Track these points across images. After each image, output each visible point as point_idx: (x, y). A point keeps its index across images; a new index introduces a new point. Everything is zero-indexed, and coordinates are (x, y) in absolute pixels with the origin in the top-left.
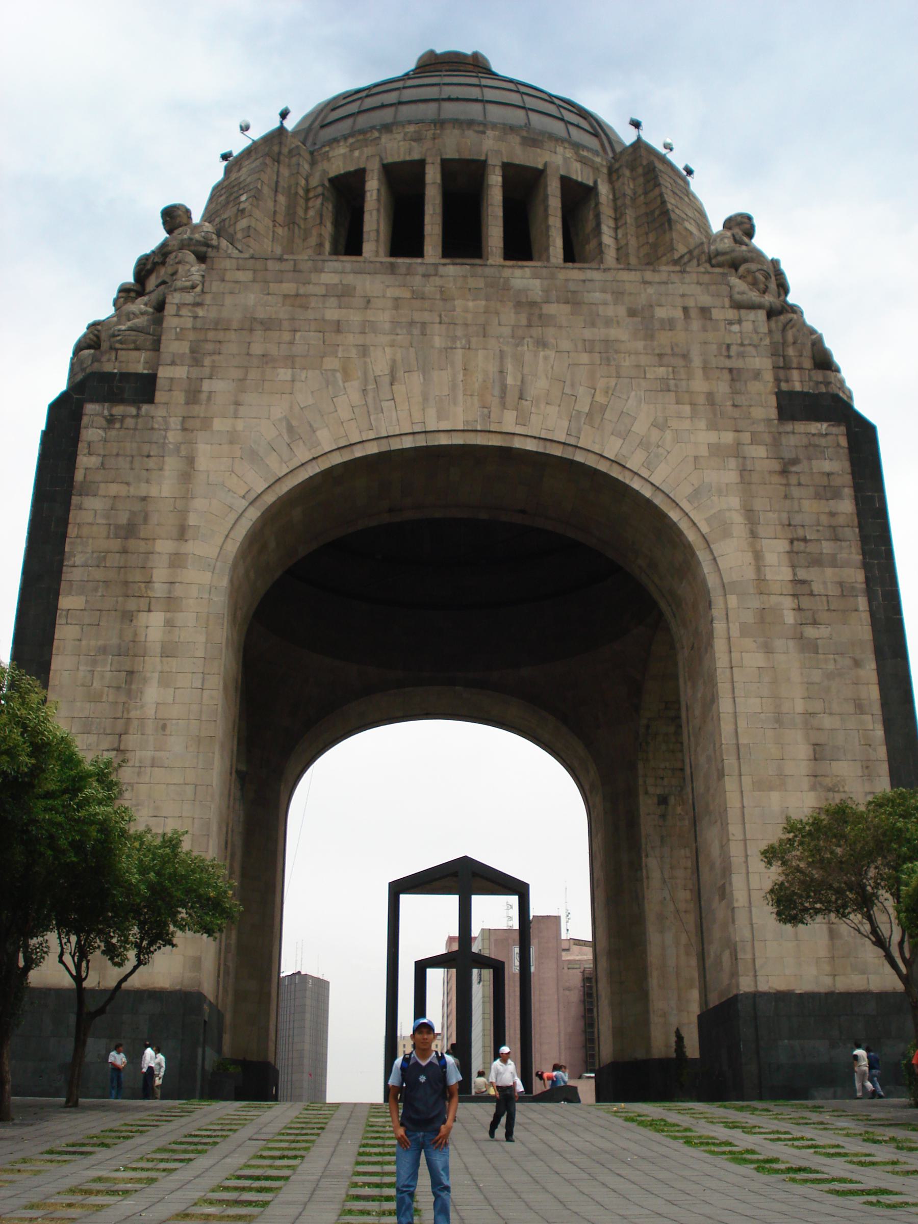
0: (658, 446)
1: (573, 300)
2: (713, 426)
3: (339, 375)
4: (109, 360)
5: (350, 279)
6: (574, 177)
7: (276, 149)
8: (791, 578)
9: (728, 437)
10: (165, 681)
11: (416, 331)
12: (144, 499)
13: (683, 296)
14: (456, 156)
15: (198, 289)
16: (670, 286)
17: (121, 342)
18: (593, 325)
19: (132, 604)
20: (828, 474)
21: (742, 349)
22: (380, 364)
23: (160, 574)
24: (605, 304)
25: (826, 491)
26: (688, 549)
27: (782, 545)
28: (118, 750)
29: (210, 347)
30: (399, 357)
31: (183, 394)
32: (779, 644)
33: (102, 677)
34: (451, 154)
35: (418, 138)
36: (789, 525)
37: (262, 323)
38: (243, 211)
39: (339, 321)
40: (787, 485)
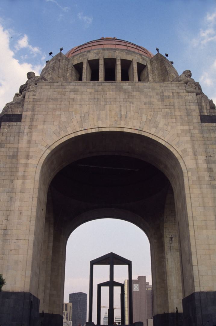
0: (166, 130)
2: (182, 124)
5: (77, 87)
6: (141, 63)
7: (59, 58)
8: (207, 167)
9: (187, 128)
11: (96, 100)
14: (108, 58)
26: (176, 160)
32: (204, 186)
35: (98, 54)
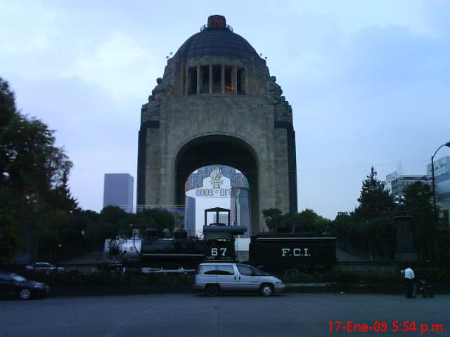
9: (264, 132)
22: (200, 119)
23: (163, 162)
25: (283, 142)
27: (273, 153)
34: (215, 64)
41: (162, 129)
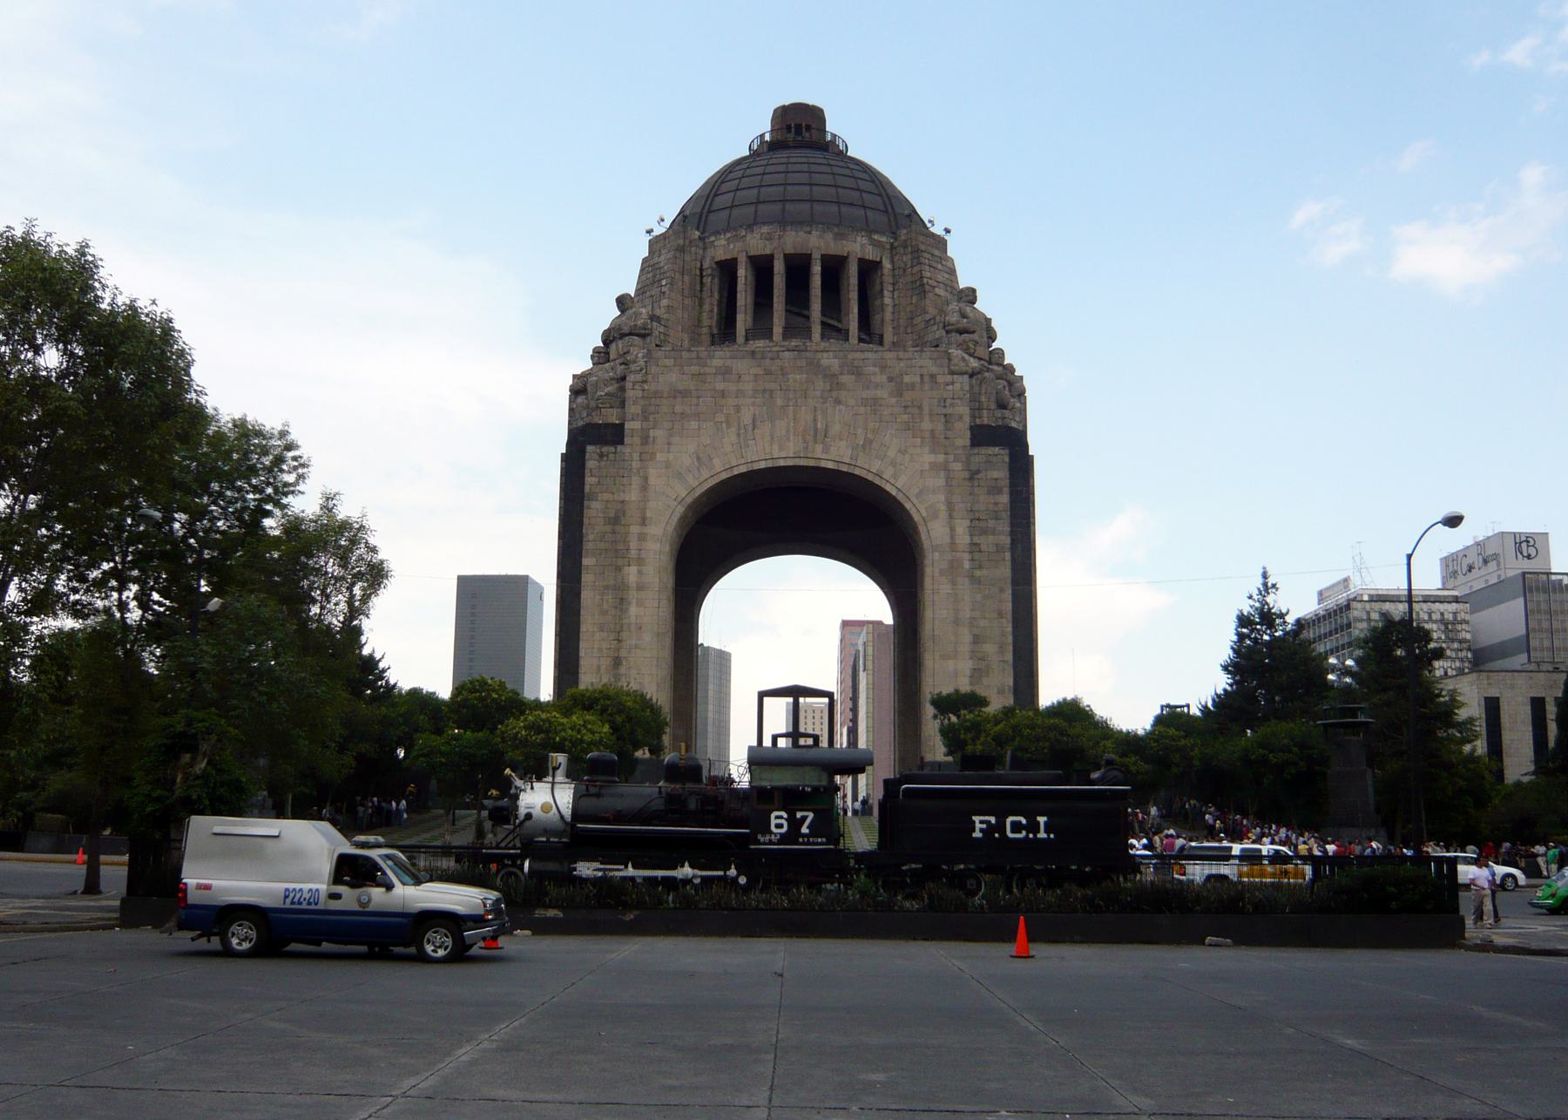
0: (901, 465)
1: (857, 372)
2: (933, 452)
3: (724, 425)
4: (597, 415)
5: (729, 363)
6: (867, 258)
8: (969, 542)
9: (941, 458)
10: (640, 604)
11: (767, 395)
12: (622, 502)
13: (921, 367)
14: (792, 252)
15: (644, 371)
16: (914, 361)
17: (602, 403)
18: (868, 388)
19: (620, 562)
20: (996, 479)
21: (953, 401)
22: (747, 418)
23: (633, 544)
24: (874, 374)
25: (994, 490)
27: (967, 523)
28: (618, 640)
29: (652, 409)
30: (757, 412)
31: (639, 438)
33: (607, 602)
34: (790, 250)
35: (769, 238)
36: (971, 511)
37: (680, 392)
38: (664, 293)
39: (723, 390)
40: (973, 486)
41: (631, 447)
